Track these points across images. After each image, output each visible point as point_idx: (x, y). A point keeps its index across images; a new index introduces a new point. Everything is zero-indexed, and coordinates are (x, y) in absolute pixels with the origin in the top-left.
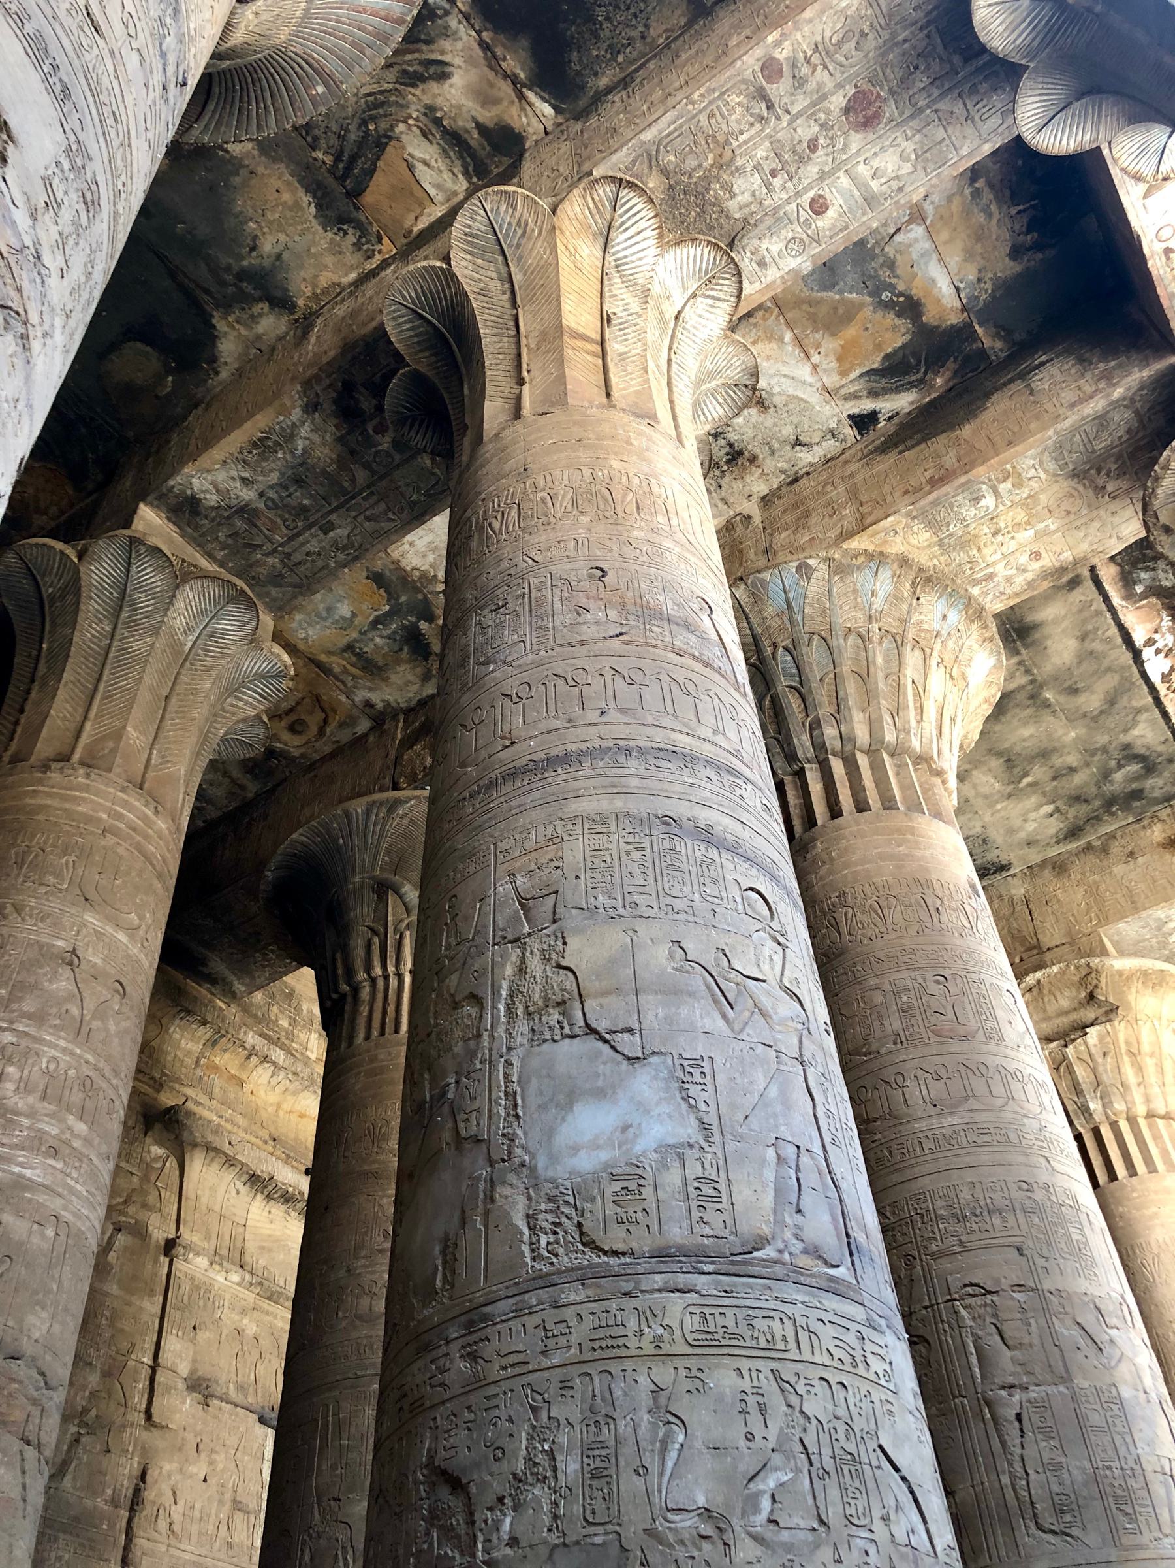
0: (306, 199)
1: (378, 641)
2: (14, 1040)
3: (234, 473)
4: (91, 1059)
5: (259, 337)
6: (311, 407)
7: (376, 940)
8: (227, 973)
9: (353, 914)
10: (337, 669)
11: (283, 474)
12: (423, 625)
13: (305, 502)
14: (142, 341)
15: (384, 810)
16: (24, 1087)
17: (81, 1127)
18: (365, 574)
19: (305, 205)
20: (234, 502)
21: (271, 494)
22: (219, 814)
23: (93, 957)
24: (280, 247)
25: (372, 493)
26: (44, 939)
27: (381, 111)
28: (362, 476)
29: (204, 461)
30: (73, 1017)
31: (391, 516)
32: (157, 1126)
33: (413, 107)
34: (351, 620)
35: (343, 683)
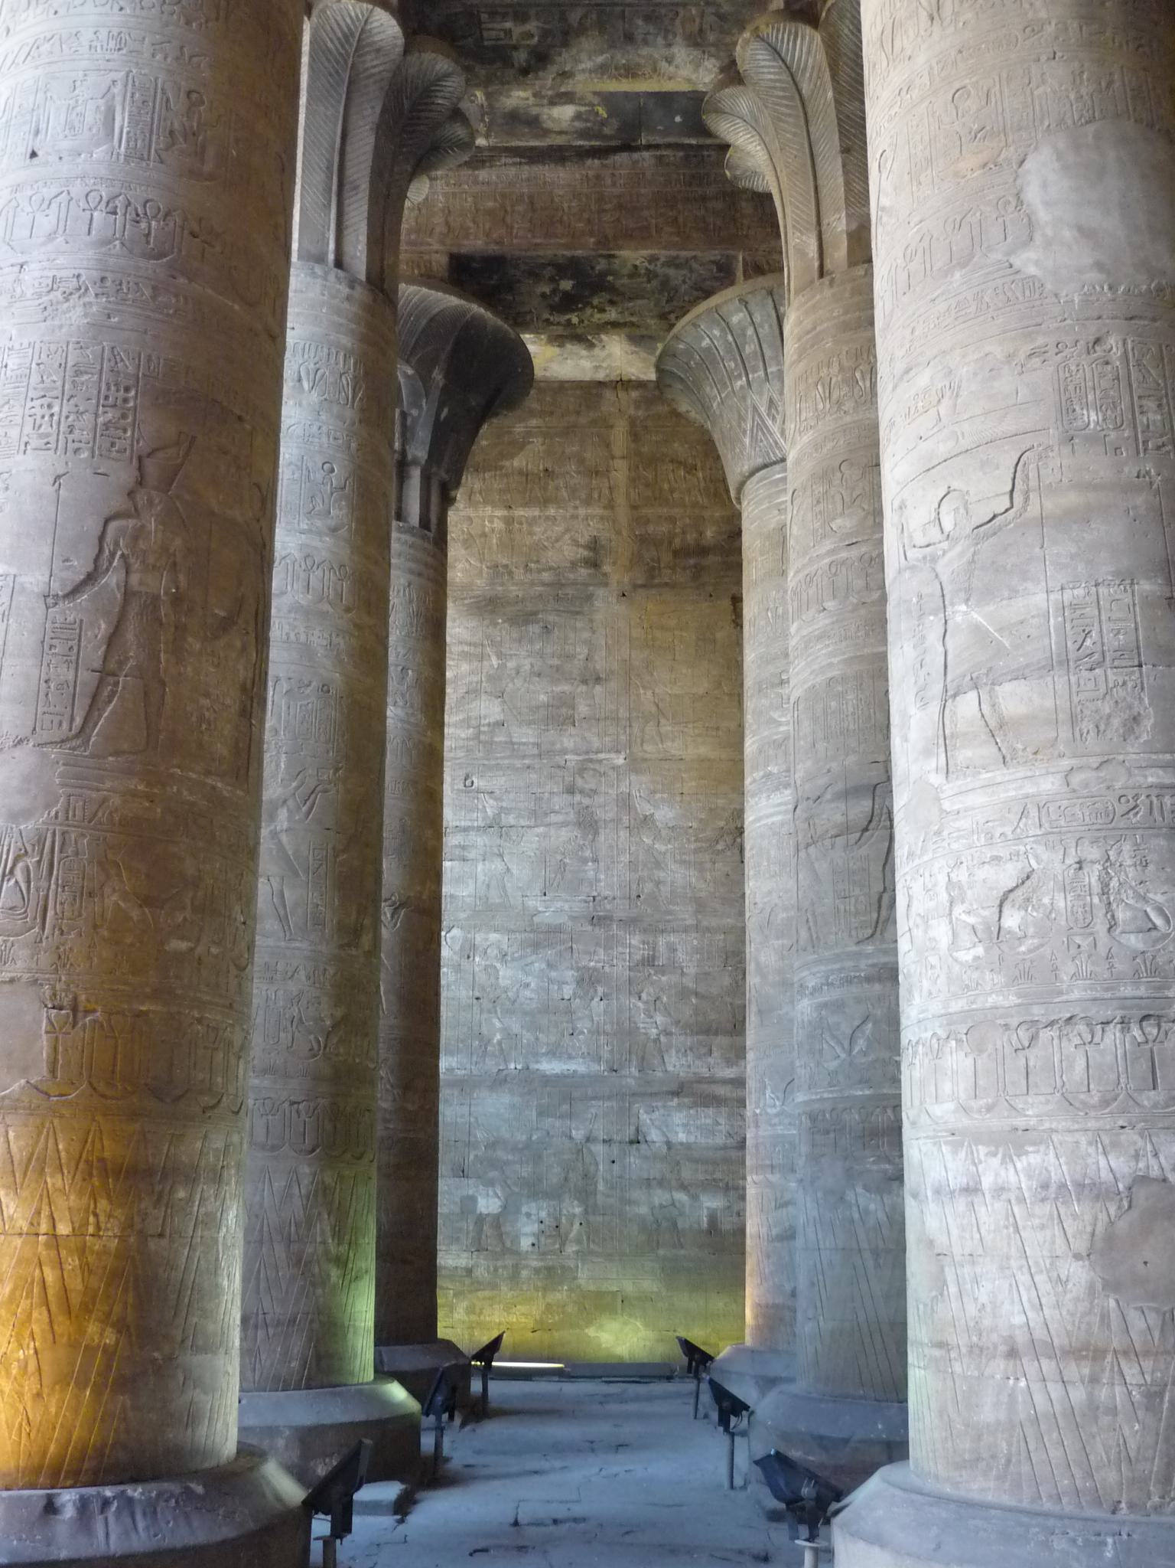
6: (565, 75)
13: (640, 22)
21: (660, 41)
28: (574, 17)
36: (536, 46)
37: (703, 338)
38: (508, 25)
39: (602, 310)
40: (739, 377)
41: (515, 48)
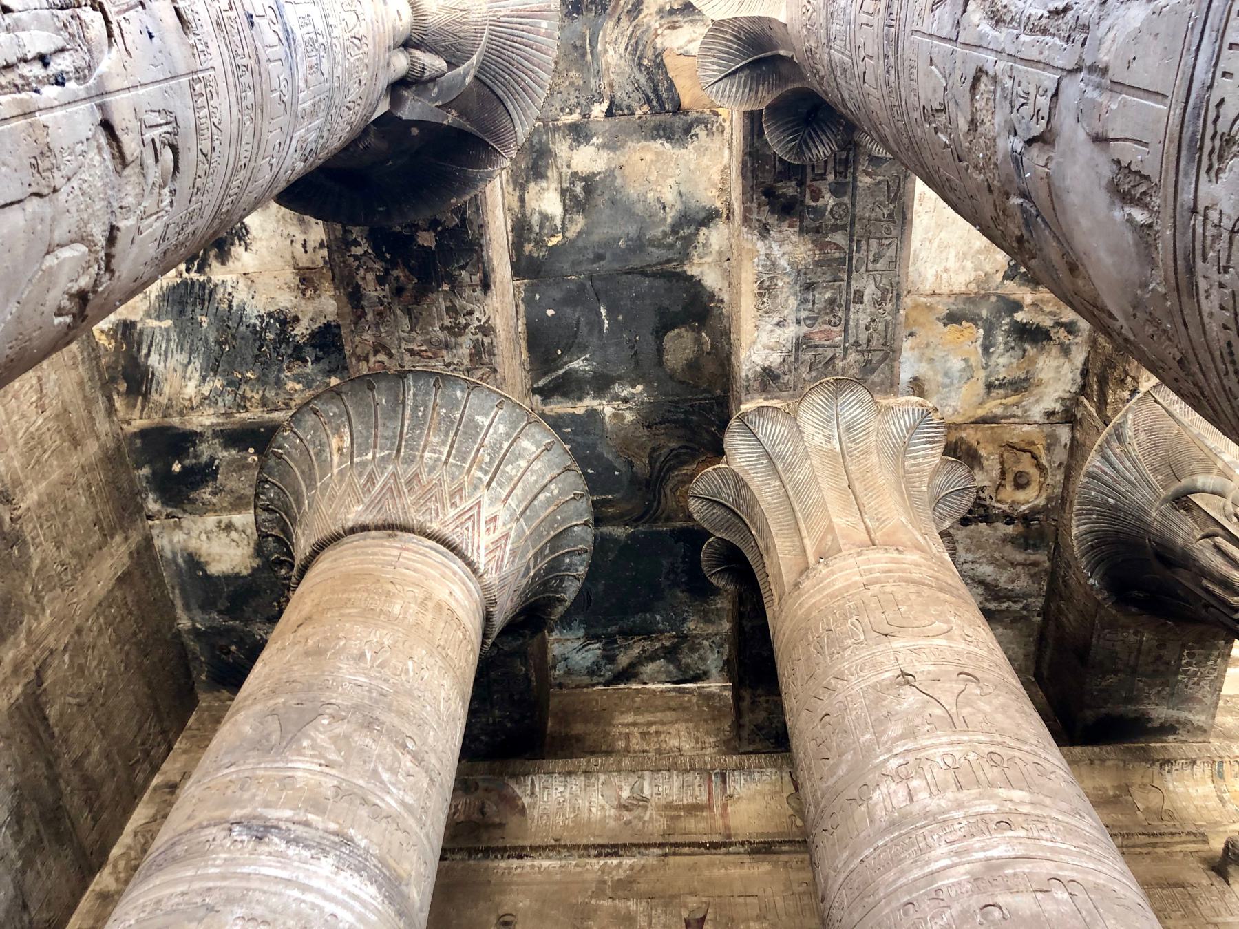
0: (658, 145)
1: (1005, 363)
2: (901, 761)
3: (769, 327)
4: (982, 738)
5: (720, 253)
6: (764, 231)
7: (1219, 539)
8: (1174, 713)
9: (1180, 541)
10: (999, 411)
11: (795, 294)
12: (1019, 316)
13: (828, 295)
14: (672, 329)
15: (1115, 445)
16: (937, 789)
17: (1017, 795)
18: (941, 325)
19: (661, 148)
20: (789, 346)
21: (803, 314)
22: (1042, 600)
23: (921, 667)
24: (675, 187)
25: (859, 242)
26: (873, 680)
27: (641, 48)
28: (839, 238)
29: (745, 339)
30: (939, 717)
31: (886, 242)
32: (1231, 869)
33: (652, 23)
34: (970, 366)
35: (1014, 416)
36: (802, 202)
37: (486, 415)
38: (831, 178)
39: (380, 281)
40: (486, 473)
41: (801, 184)
